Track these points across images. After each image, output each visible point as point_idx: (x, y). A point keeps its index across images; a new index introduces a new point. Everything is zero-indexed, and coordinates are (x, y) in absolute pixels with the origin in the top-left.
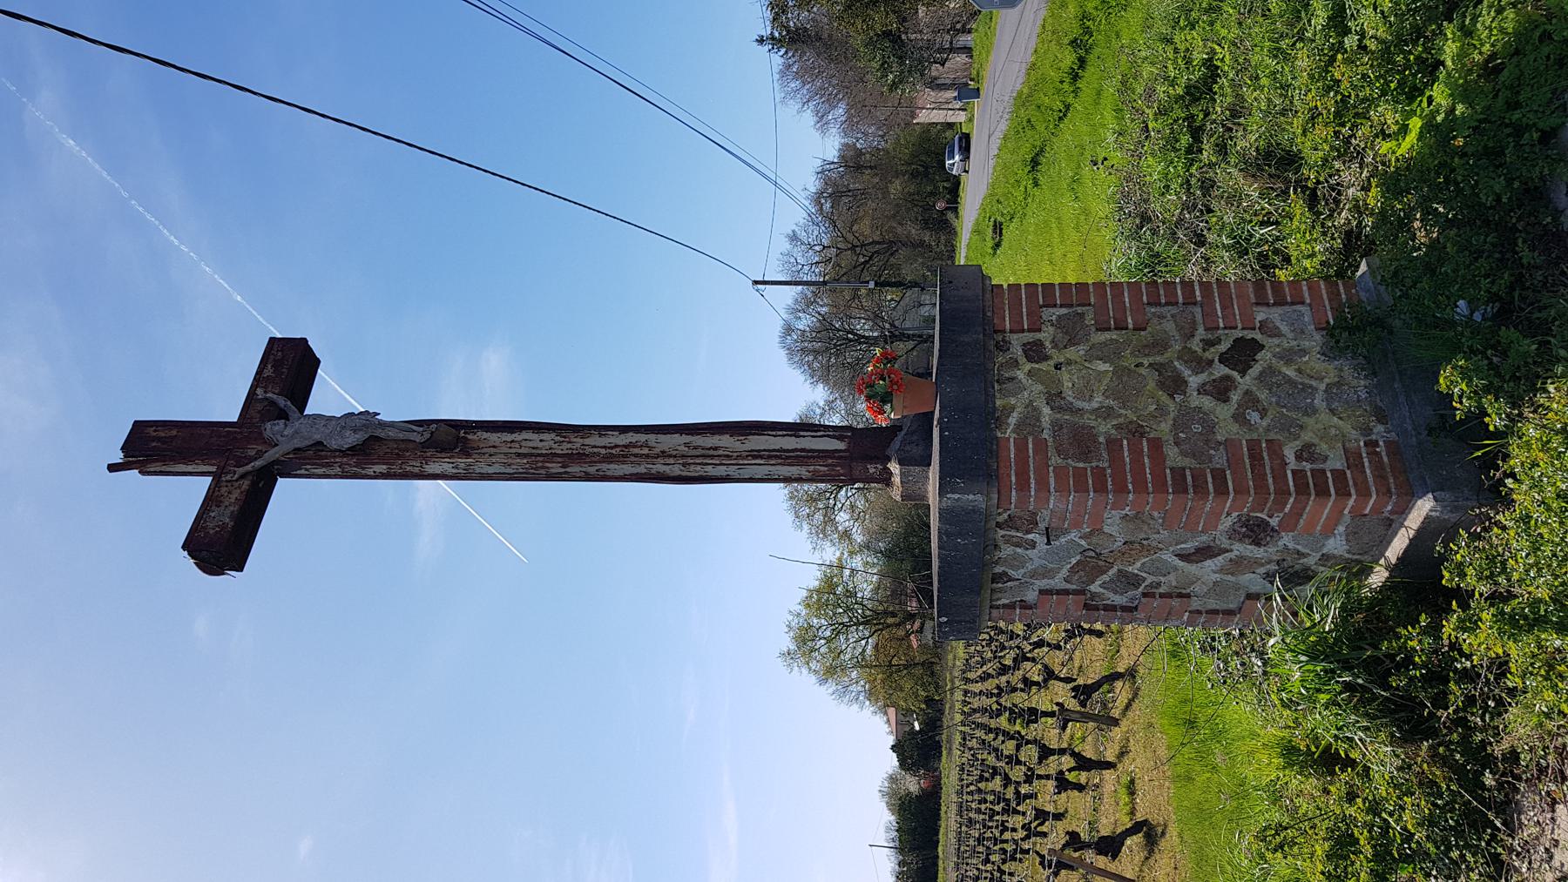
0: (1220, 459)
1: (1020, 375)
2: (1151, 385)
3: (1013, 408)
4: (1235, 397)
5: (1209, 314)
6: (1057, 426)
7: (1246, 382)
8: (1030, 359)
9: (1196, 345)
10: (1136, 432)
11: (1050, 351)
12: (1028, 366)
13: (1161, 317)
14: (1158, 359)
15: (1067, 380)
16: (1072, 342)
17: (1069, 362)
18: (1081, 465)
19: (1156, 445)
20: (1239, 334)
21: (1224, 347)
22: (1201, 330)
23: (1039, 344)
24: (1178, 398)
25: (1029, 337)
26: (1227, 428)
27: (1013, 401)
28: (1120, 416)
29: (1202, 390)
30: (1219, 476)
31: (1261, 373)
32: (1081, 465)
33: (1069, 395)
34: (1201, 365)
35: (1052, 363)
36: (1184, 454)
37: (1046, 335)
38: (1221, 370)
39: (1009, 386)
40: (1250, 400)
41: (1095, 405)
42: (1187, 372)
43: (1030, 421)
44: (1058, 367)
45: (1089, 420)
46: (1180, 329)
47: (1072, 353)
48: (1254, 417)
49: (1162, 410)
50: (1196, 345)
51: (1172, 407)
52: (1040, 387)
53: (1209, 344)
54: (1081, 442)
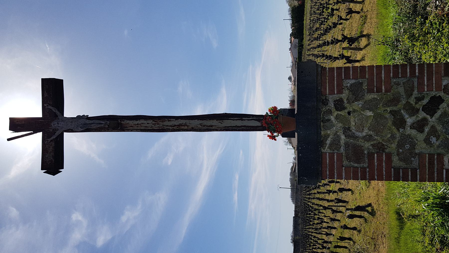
0: (415, 163)
1: (332, 118)
2: (390, 123)
3: (329, 136)
4: (427, 130)
5: (420, 84)
6: (347, 144)
7: (432, 120)
8: (337, 109)
9: (412, 101)
10: (380, 148)
11: (346, 105)
12: (336, 113)
13: (398, 84)
14: (395, 108)
15: (353, 121)
16: (356, 100)
17: (354, 111)
18: (356, 165)
19: (389, 156)
20: (433, 93)
21: (425, 101)
22: (416, 92)
23: (341, 100)
24: (401, 130)
25: (336, 97)
26: (421, 147)
27: (329, 132)
28: (375, 140)
29: (412, 127)
30: (414, 171)
31: (441, 116)
32: (356, 165)
33: (353, 128)
34: (413, 111)
35: (346, 111)
36: (400, 160)
37: (345, 95)
38: (422, 115)
39: (327, 124)
40: (433, 131)
41: (364, 134)
42: (407, 116)
43: (336, 144)
44: (349, 113)
45: (361, 142)
46: (406, 91)
47: (357, 105)
48: (433, 140)
49: (393, 137)
50: (412, 101)
51: (398, 135)
52: (340, 125)
53: (418, 99)
54: (356, 153)
